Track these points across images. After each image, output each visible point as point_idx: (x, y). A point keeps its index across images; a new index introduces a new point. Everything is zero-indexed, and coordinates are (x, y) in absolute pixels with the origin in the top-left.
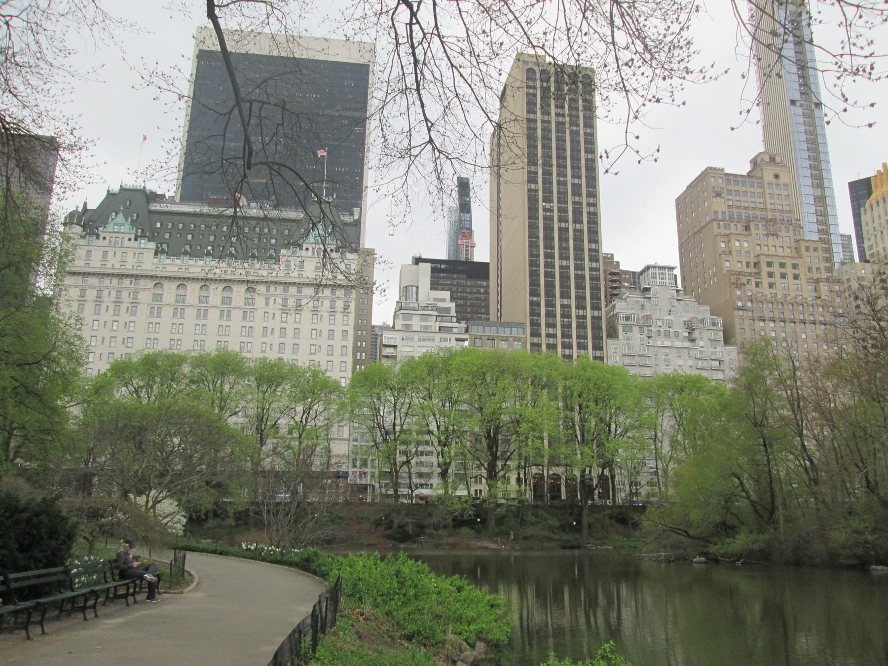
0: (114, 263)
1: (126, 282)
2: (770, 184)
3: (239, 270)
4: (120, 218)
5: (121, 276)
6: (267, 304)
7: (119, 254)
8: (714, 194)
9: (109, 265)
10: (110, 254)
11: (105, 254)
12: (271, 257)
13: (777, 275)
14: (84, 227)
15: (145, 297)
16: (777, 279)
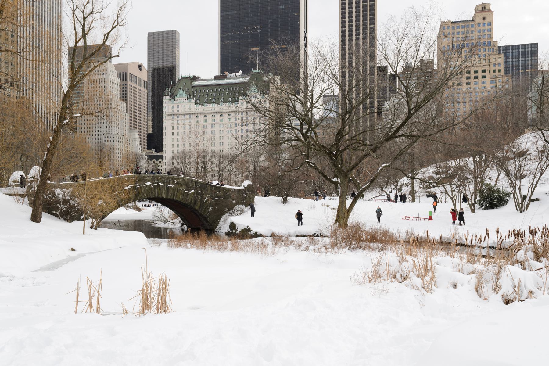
0: (181, 109)
1: (186, 116)
2: (479, 25)
3: (225, 107)
4: (181, 91)
5: (184, 114)
6: (236, 120)
7: (183, 106)
8: (444, 37)
9: (180, 111)
10: (180, 106)
11: (178, 107)
12: (236, 101)
13: (472, 78)
14: (170, 96)
15: (193, 121)
16: (472, 80)
